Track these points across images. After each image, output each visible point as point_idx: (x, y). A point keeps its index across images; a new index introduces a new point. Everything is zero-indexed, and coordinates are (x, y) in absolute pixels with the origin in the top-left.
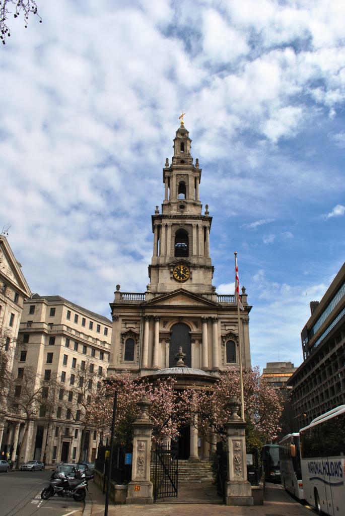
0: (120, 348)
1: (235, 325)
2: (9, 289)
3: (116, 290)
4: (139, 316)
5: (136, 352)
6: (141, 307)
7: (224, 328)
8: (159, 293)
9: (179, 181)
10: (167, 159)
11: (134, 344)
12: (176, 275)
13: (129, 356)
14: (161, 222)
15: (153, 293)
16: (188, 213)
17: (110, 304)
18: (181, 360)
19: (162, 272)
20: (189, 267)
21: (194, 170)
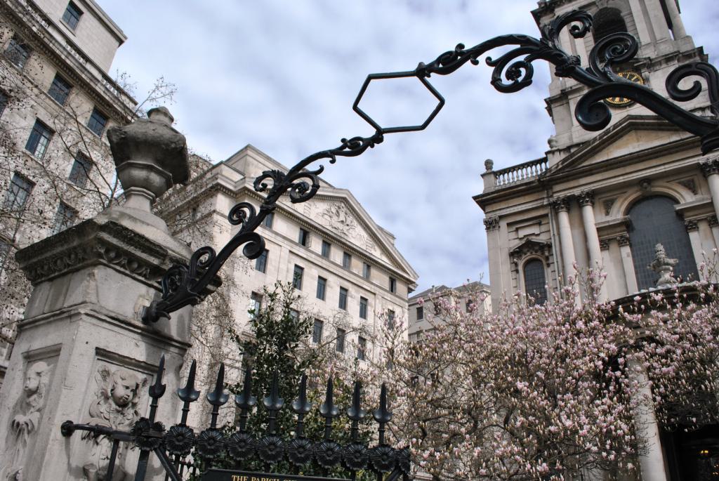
0: (513, 283)
2: (374, 272)
3: (484, 170)
4: (542, 207)
6: (543, 184)
11: (543, 268)
14: (555, 15)
17: (475, 198)
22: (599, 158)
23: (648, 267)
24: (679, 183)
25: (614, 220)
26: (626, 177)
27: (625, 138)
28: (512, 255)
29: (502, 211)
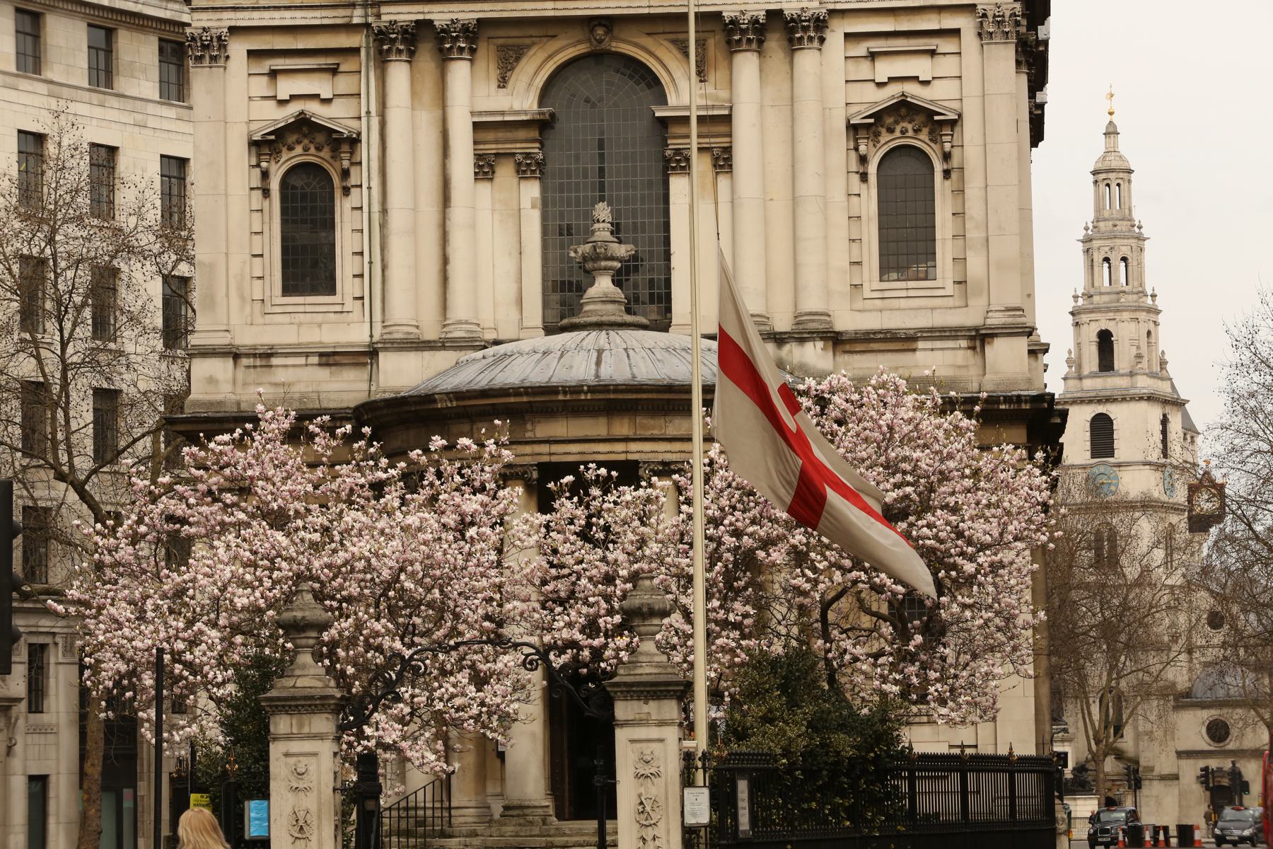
1: (932, 53)
4: (349, 27)
5: (346, 240)
7: (864, 70)
18: (604, 285)
23: (572, 254)
25: (518, 113)
28: (254, 144)
29: (240, 15)
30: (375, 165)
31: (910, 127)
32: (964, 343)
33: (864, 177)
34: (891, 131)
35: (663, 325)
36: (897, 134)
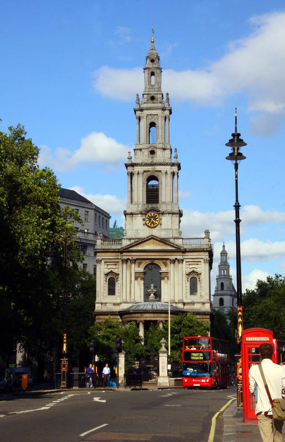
1: (198, 264)
4: (118, 259)
7: (188, 266)
8: (134, 239)
9: (149, 122)
10: (138, 95)
12: (148, 222)
13: (112, 291)
15: (129, 239)
16: (158, 159)
18: (152, 295)
19: (135, 219)
20: (159, 214)
21: (164, 109)
22: (140, 248)
24: (162, 262)
26: (147, 257)
27: (149, 241)
30: (121, 278)
31: (194, 274)
32: (201, 304)
33: (188, 281)
34: (192, 275)
35: (160, 301)
36: (193, 275)
